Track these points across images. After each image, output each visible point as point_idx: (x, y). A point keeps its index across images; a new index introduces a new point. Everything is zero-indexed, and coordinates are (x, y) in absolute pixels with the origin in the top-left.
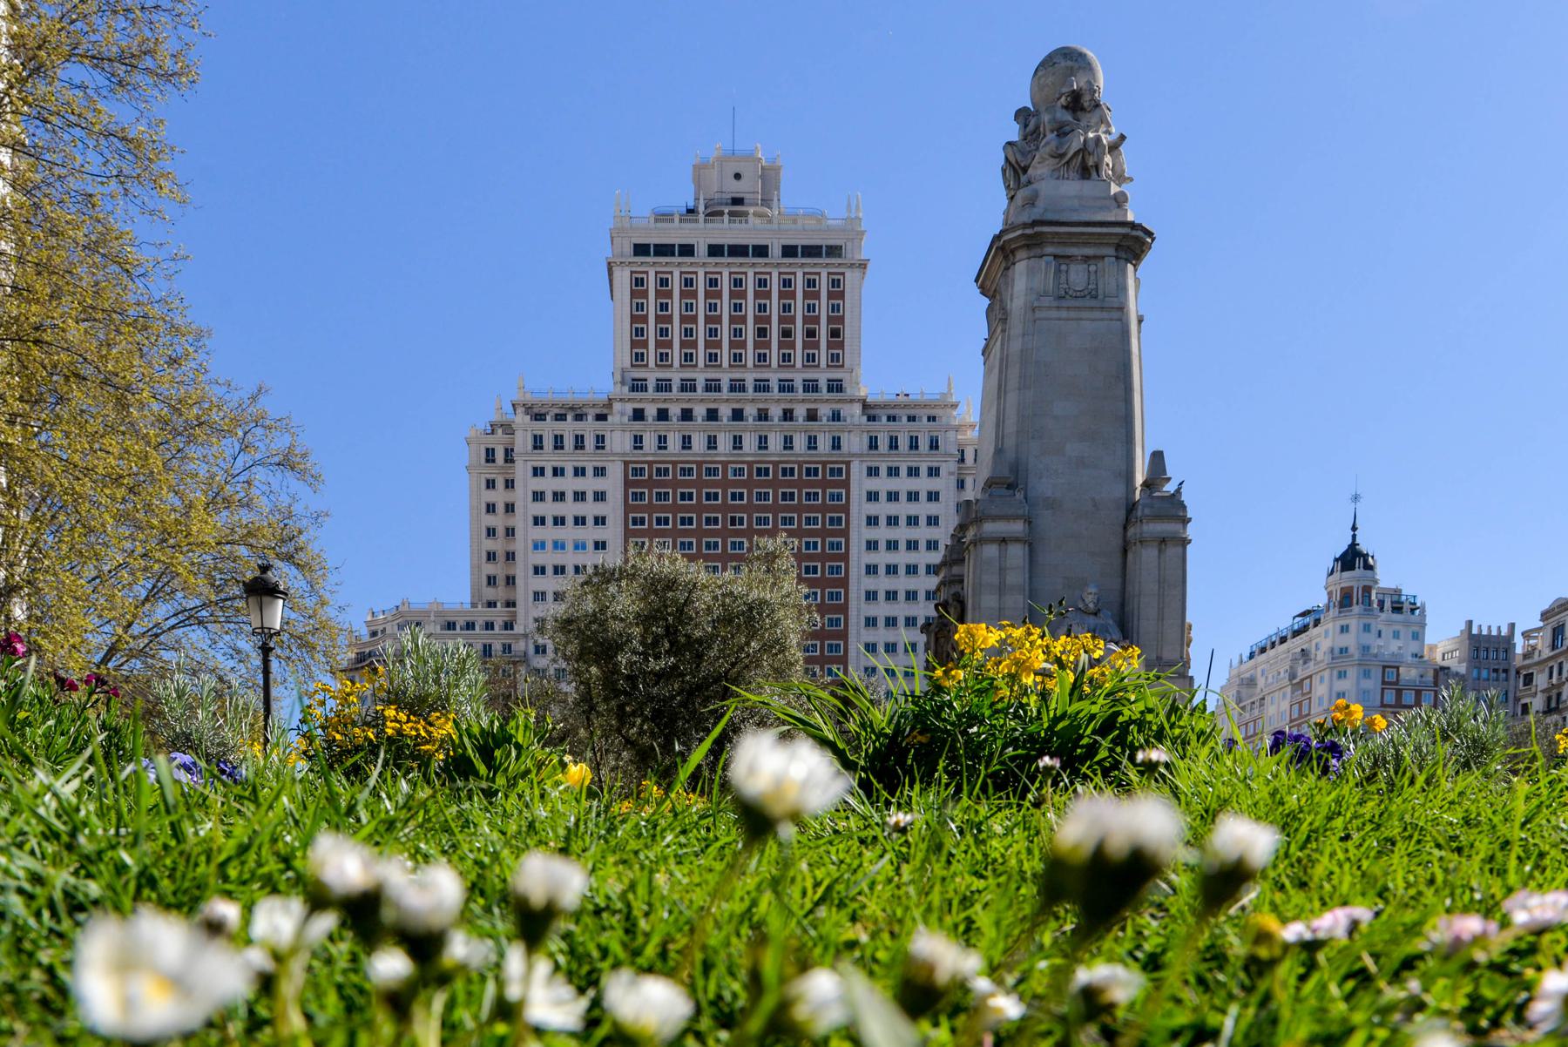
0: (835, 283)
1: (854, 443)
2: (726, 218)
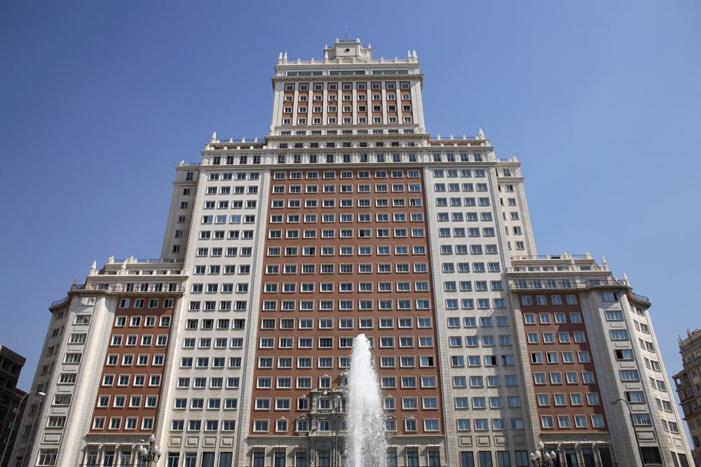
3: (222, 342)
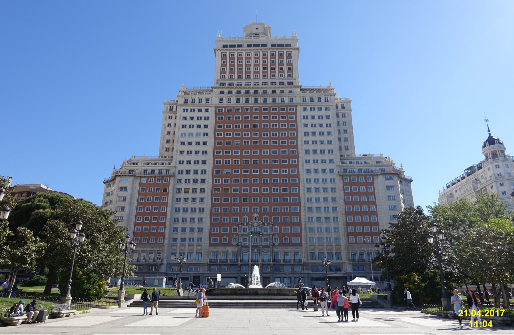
0: (289, 54)
1: (298, 100)
2: (253, 38)
3: (194, 200)
